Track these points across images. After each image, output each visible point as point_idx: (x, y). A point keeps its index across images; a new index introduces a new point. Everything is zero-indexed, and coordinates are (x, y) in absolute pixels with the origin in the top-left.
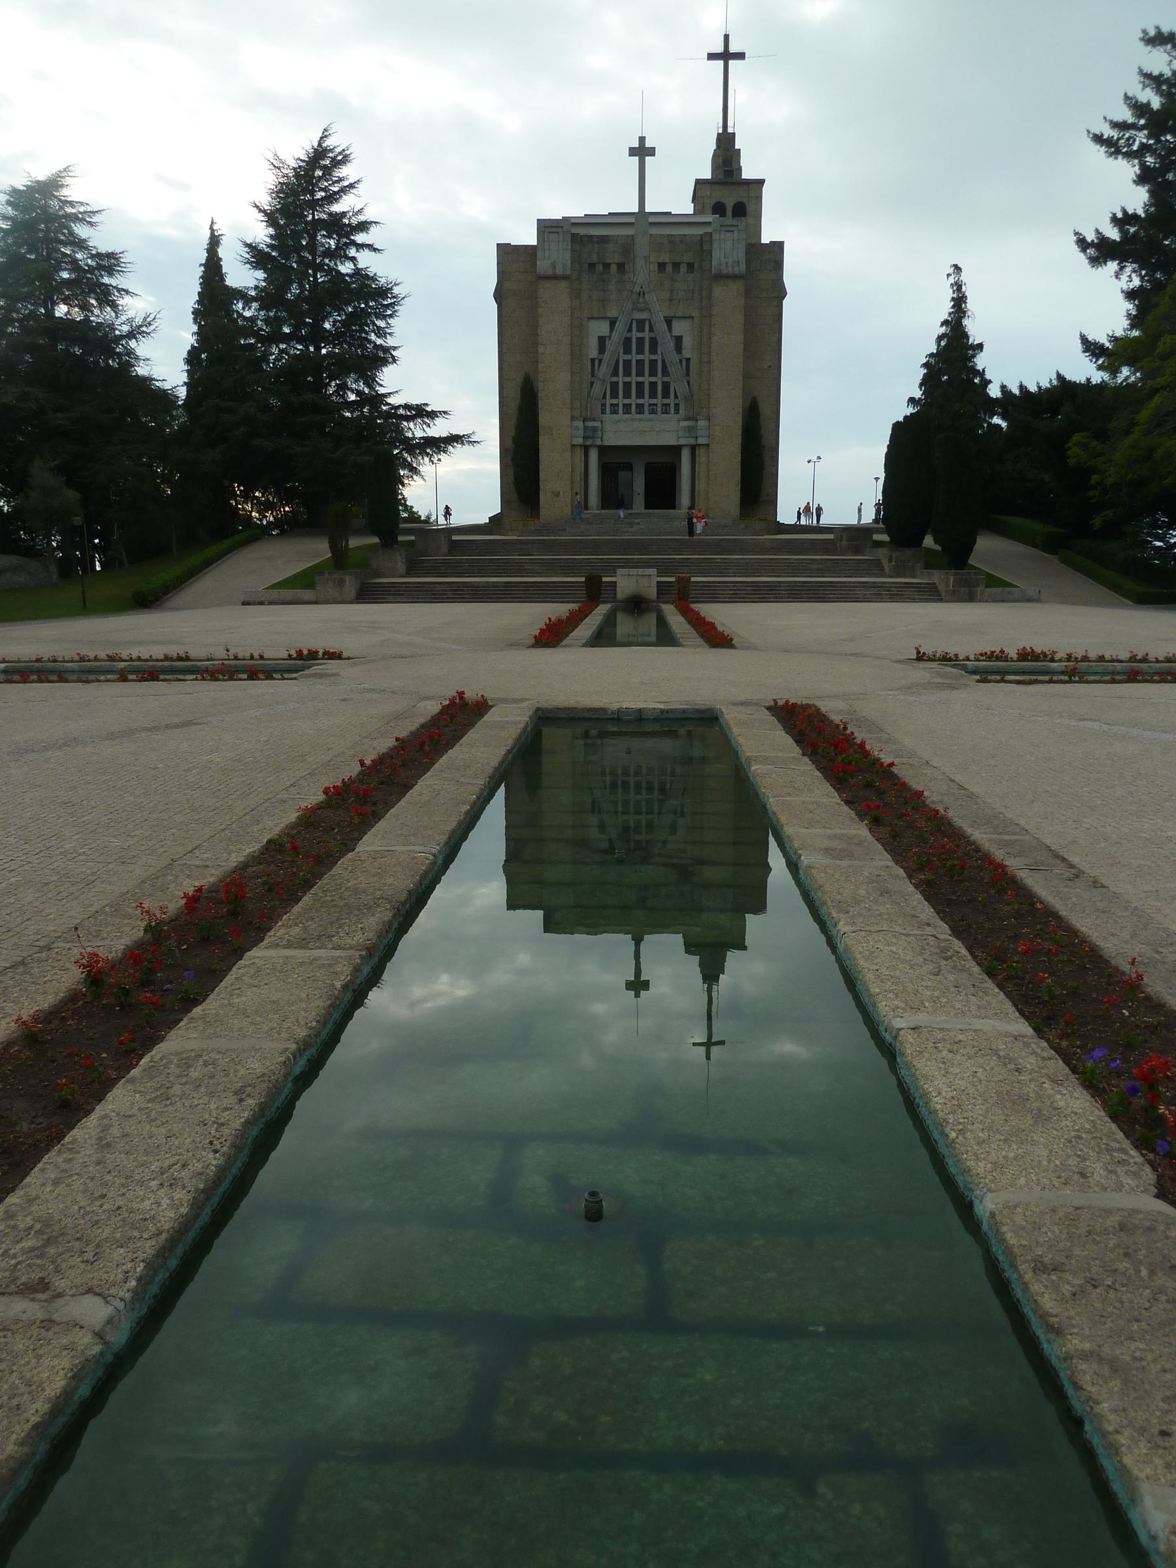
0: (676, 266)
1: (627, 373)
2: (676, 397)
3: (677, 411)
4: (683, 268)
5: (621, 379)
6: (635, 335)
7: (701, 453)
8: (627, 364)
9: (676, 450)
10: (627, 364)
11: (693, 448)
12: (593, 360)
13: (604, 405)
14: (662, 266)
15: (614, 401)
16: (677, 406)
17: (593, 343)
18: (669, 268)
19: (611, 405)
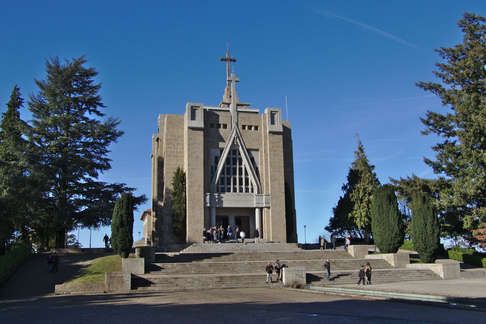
0: (250, 127)
1: (229, 173)
2: (252, 185)
3: (252, 191)
4: (253, 128)
5: (226, 176)
6: (232, 156)
7: (265, 210)
8: (228, 169)
9: (254, 209)
10: (228, 169)
11: (261, 209)
12: (212, 167)
13: (218, 188)
14: (244, 127)
15: (223, 186)
16: (252, 189)
17: (213, 159)
18: (246, 128)
19: (221, 188)
